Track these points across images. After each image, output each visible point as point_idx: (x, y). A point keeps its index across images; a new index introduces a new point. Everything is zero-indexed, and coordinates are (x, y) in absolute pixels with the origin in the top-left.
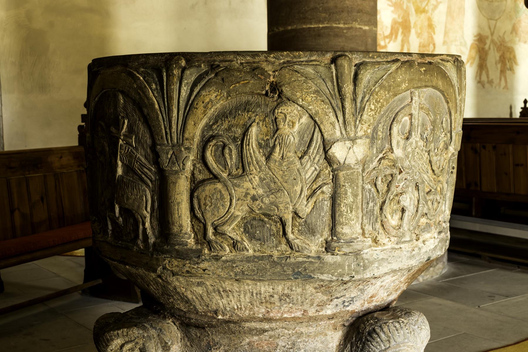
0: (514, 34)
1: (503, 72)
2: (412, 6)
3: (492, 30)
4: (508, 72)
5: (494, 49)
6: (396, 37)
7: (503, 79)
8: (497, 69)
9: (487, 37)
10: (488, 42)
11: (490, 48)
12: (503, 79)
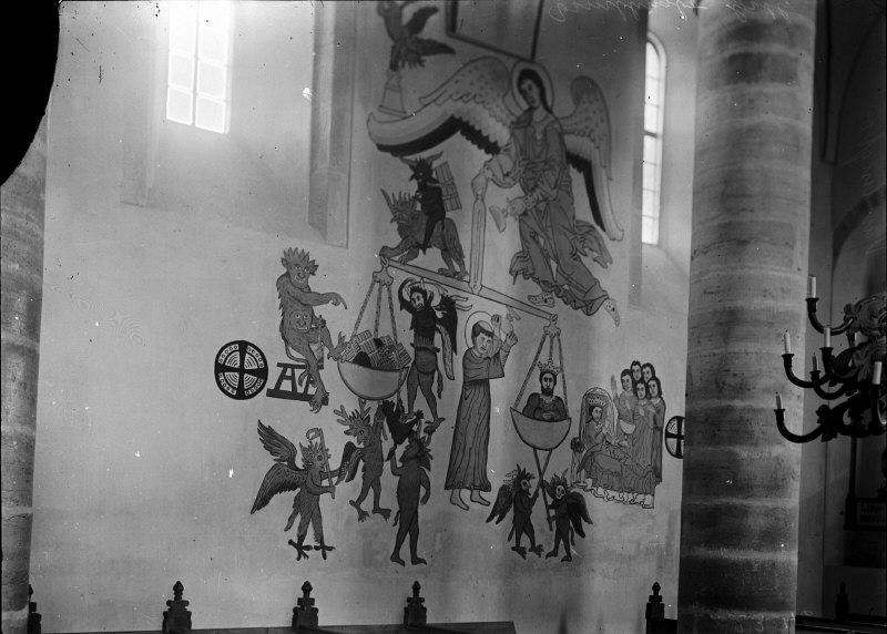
1: (561, 534)
2: (385, 423)
6: (352, 477)
10: (534, 483)
11: (536, 494)
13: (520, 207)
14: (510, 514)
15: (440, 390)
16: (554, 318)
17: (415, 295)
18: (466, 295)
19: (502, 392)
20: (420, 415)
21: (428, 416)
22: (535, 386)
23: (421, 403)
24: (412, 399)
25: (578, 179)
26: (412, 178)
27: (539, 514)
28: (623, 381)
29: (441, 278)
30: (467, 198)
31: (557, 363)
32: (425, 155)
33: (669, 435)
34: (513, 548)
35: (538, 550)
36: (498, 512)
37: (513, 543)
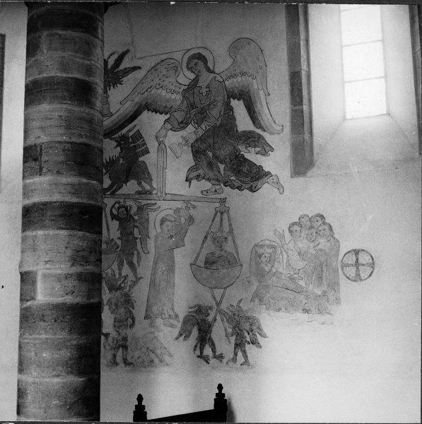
0: (257, 301)
1: (239, 345)
3: (218, 299)
4: (250, 348)
5: (222, 320)
7: (240, 354)
8: (229, 342)
9: (211, 308)
12: (240, 354)
13: (193, 138)
14: (195, 332)
15: (139, 258)
16: (223, 201)
17: (121, 210)
18: (154, 202)
19: (182, 258)
20: (126, 277)
21: (131, 277)
22: (210, 247)
23: (126, 270)
24: (120, 269)
25: (239, 107)
26: (117, 146)
27: (219, 332)
28: (290, 231)
29: (137, 196)
30: (152, 145)
31: (226, 229)
32: (124, 131)
33: (344, 266)
34: (199, 357)
35: (220, 357)
36: (185, 334)
37: (198, 352)
